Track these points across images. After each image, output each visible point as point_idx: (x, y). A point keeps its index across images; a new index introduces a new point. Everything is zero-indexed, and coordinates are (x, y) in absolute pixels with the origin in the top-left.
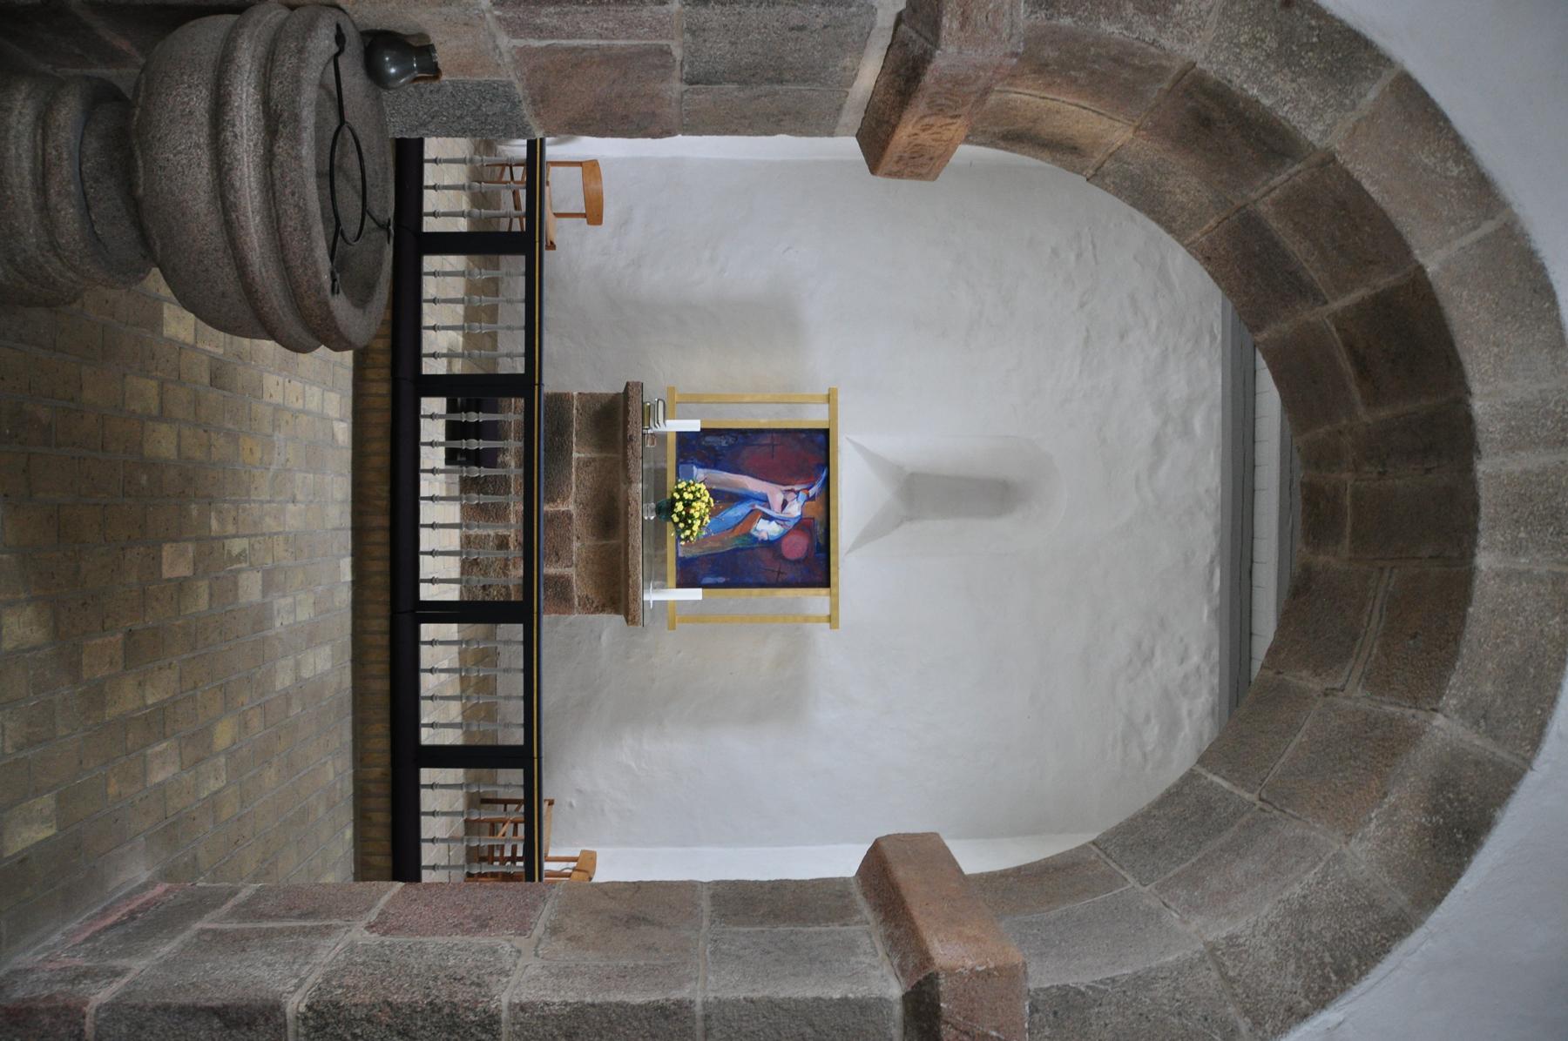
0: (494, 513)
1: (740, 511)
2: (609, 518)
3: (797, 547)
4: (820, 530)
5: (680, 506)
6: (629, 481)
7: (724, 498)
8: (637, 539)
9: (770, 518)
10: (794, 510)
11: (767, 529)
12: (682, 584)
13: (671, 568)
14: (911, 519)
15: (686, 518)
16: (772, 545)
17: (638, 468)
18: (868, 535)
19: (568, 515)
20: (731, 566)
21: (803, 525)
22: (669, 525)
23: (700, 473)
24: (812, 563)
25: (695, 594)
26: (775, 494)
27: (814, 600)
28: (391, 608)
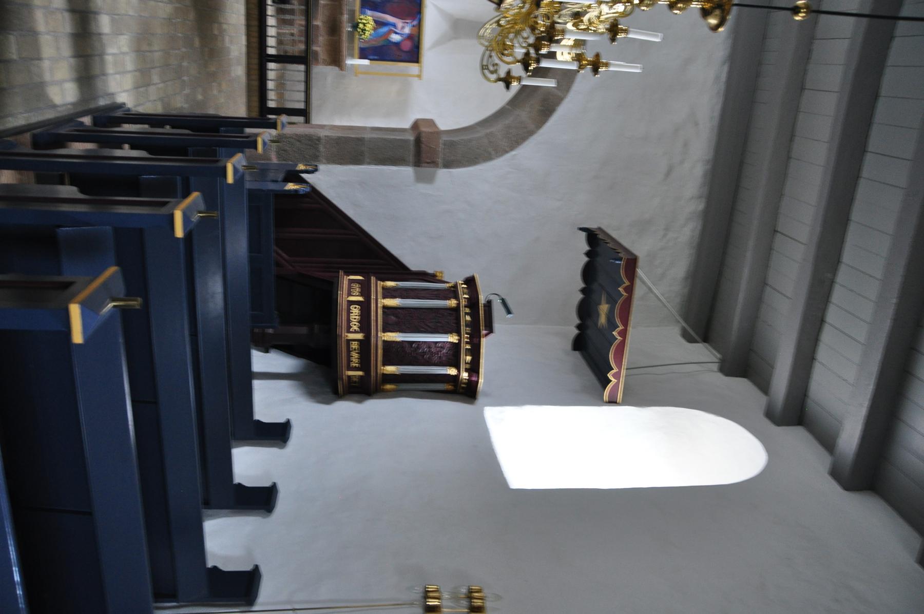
0: (290, 23)
1: (384, 30)
2: (334, 28)
3: (407, 46)
4: (416, 39)
5: (361, 26)
6: (342, 14)
7: (379, 23)
8: (345, 37)
9: (396, 33)
10: (407, 30)
11: (395, 38)
12: (361, 58)
13: (357, 51)
14: (456, 38)
15: (364, 30)
16: (397, 44)
17: (345, 9)
18: (438, 43)
19: (317, 26)
20: (380, 52)
21: (410, 37)
22: (356, 33)
23: (369, 12)
24: (411, 52)
25: (366, 62)
26: (399, 23)
27: (413, 68)
28: (259, 58)
